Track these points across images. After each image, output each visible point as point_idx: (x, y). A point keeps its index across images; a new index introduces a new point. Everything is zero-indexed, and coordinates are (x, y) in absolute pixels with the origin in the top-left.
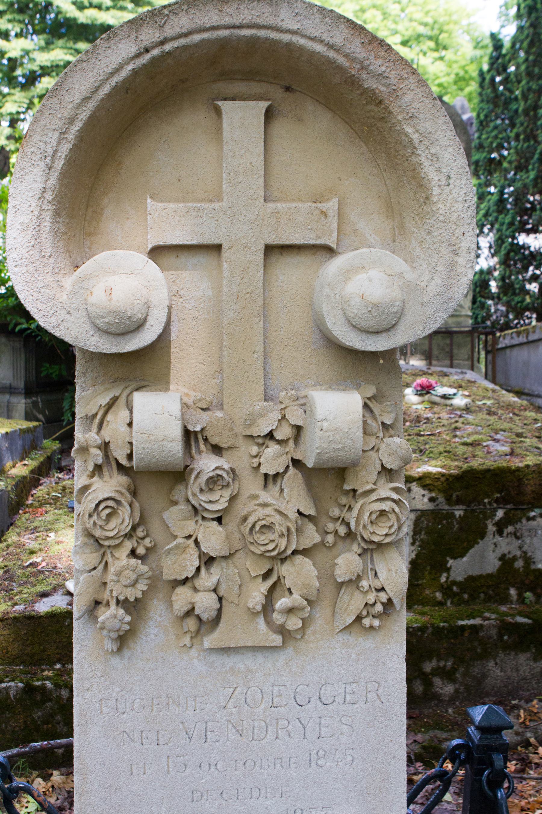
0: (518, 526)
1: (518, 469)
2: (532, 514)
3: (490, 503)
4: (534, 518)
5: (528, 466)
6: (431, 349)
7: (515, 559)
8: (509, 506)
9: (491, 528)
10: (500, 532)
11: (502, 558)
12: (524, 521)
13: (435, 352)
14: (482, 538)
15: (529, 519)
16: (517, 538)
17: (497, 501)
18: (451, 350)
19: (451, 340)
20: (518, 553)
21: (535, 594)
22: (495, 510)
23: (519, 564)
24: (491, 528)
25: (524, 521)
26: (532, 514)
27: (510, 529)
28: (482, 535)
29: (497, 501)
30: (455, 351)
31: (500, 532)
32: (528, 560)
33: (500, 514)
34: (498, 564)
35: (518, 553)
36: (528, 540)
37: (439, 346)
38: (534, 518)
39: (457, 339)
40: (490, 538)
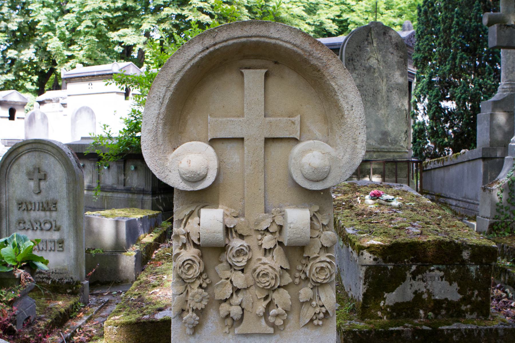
0: (424, 275)
1: (424, 243)
2: (432, 268)
3: (408, 262)
4: (433, 270)
5: (429, 241)
6: (384, 171)
7: (422, 293)
8: (419, 264)
9: (409, 276)
10: (414, 278)
11: (415, 293)
12: (427, 272)
13: (387, 173)
14: (404, 282)
15: (430, 271)
16: (424, 281)
17: (412, 260)
18: (396, 171)
19: (396, 167)
20: (425, 290)
21: (434, 313)
22: (411, 266)
23: (425, 296)
24: (409, 276)
25: (427, 272)
26: (432, 268)
27: (420, 276)
28: (404, 279)
29: (412, 260)
30: (399, 172)
31: (414, 278)
32: (430, 294)
33: (414, 268)
34: (413, 296)
35: (425, 290)
36: (430, 283)
37: (389, 169)
38: (433, 270)
39: (399, 165)
40: (408, 281)
